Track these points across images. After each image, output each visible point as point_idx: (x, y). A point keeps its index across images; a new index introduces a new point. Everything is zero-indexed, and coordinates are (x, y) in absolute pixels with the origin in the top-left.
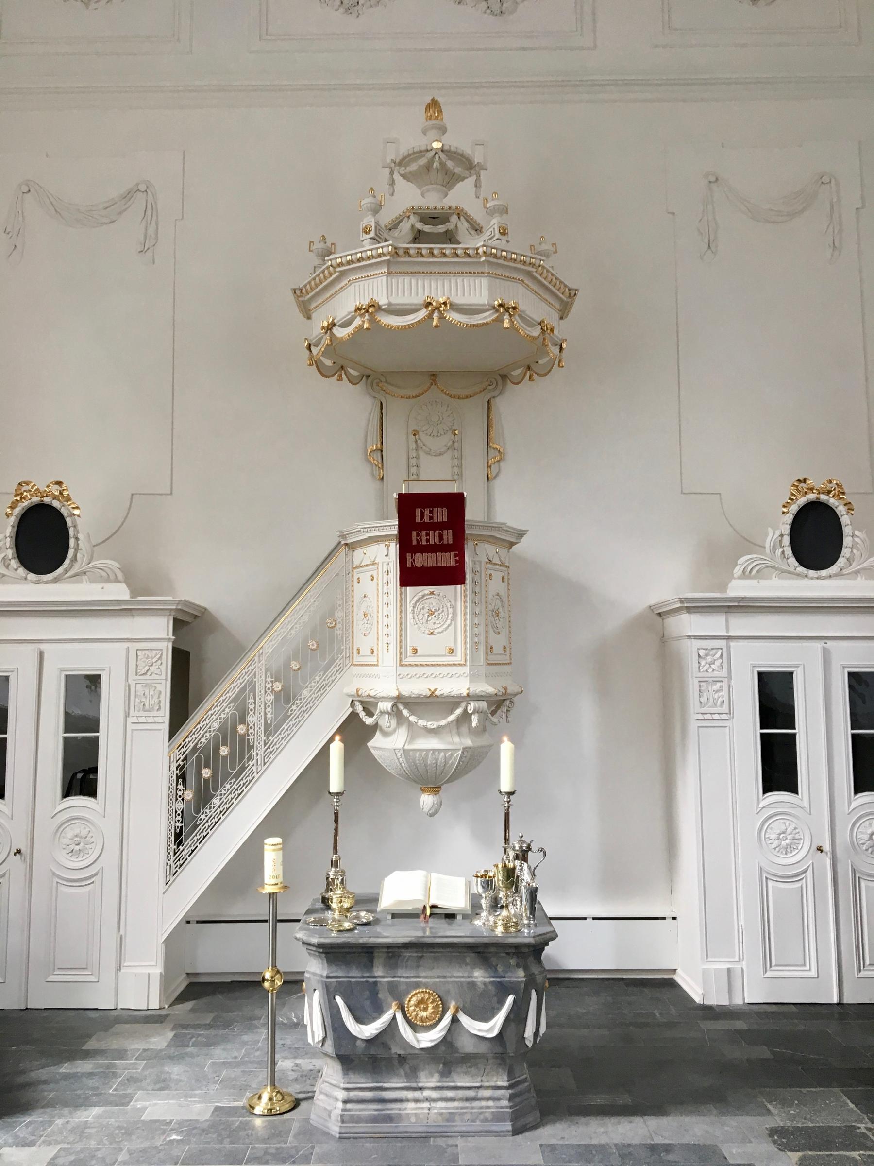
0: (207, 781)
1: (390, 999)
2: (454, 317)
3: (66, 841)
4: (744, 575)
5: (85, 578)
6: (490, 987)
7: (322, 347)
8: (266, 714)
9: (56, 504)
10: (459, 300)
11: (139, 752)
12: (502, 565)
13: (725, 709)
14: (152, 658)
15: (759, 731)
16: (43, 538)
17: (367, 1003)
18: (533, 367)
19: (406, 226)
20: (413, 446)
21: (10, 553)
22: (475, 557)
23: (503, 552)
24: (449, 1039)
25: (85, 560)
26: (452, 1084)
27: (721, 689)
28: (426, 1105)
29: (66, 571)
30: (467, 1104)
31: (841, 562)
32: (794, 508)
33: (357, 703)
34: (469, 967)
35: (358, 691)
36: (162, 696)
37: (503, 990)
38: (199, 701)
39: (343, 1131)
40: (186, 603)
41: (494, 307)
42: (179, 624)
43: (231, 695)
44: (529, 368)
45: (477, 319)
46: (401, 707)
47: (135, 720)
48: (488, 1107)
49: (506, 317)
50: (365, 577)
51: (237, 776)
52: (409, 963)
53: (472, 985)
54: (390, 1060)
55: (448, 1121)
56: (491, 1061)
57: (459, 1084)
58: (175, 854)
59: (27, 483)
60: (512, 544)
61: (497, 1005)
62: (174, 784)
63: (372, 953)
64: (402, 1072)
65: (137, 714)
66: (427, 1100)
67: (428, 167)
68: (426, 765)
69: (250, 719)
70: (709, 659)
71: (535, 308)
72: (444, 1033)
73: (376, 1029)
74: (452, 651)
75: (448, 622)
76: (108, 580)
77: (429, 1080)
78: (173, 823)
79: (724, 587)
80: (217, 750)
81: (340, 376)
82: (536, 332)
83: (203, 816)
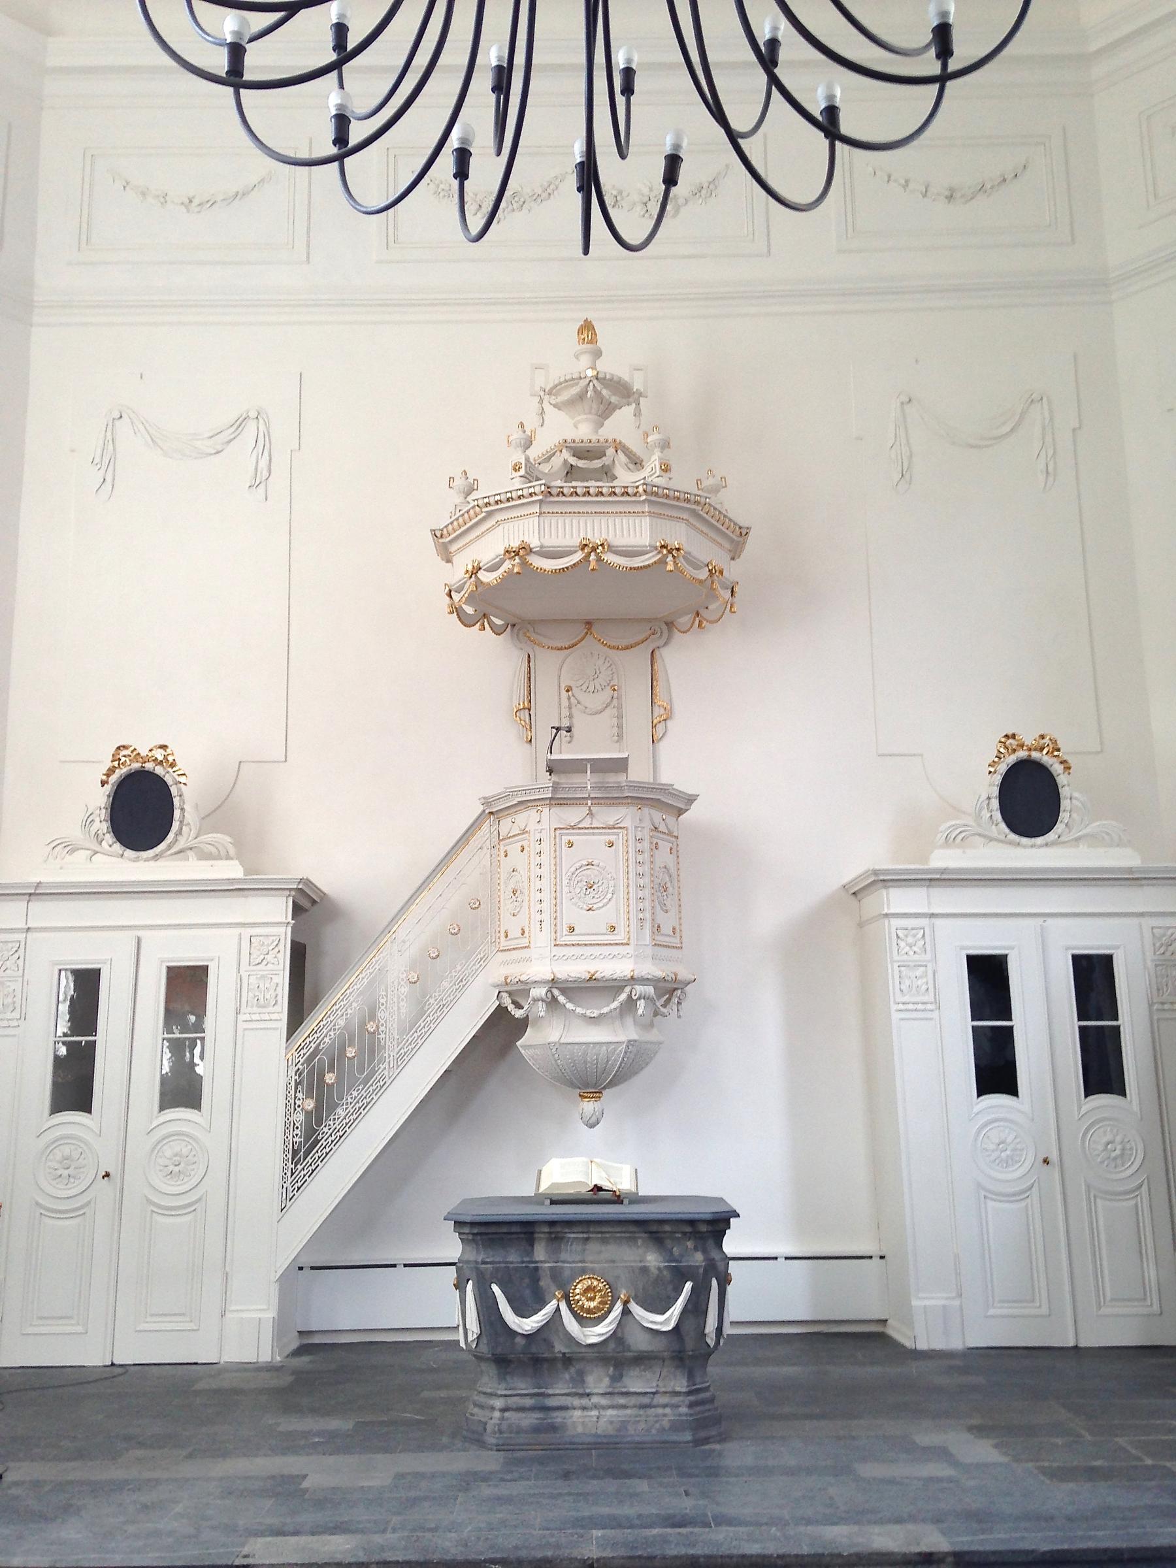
0: (331, 1086)
1: (553, 1288)
3: (161, 1161)
4: (948, 842)
5: (190, 854)
6: (665, 1273)
7: (465, 593)
8: (399, 1008)
9: (159, 770)
10: (618, 541)
12: (670, 834)
13: (930, 997)
14: (268, 945)
15: (970, 1024)
16: (141, 808)
17: (527, 1293)
18: (702, 611)
19: (557, 461)
20: (565, 703)
21: (105, 826)
23: (671, 820)
24: (619, 1335)
25: (193, 834)
26: (624, 1390)
27: (925, 975)
28: (594, 1413)
29: (169, 847)
30: (642, 1412)
31: (1059, 827)
32: (1003, 768)
33: (505, 995)
34: (641, 1251)
35: (506, 978)
36: (279, 989)
37: (680, 1275)
38: (315, 1003)
39: (501, 1442)
40: (307, 882)
41: (656, 548)
42: (297, 909)
44: (698, 614)
45: (638, 562)
46: (556, 992)
47: (247, 1017)
48: (665, 1415)
49: (670, 558)
50: (514, 849)
51: (366, 1082)
52: (574, 1246)
53: (644, 1270)
54: (552, 1361)
55: (619, 1430)
56: (667, 1363)
57: (632, 1390)
58: (292, 1174)
59: (125, 747)
60: (680, 812)
61: (673, 1295)
62: (293, 1092)
63: (533, 1233)
64: (567, 1376)
65: (249, 1010)
66: (596, 1407)
67: (582, 396)
68: (585, 1062)
70: (910, 940)
71: (703, 548)
72: (614, 1326)
73: (538, 1322)
74: (613, 928)
75: (609, 896)
76: (218, 857)
77: (598, 1381)
78: (290, 1137)
79: (926, 859)
80: (342, 1050)
81: (483, 625)
82: (703, 574)
83: (326, 1130)
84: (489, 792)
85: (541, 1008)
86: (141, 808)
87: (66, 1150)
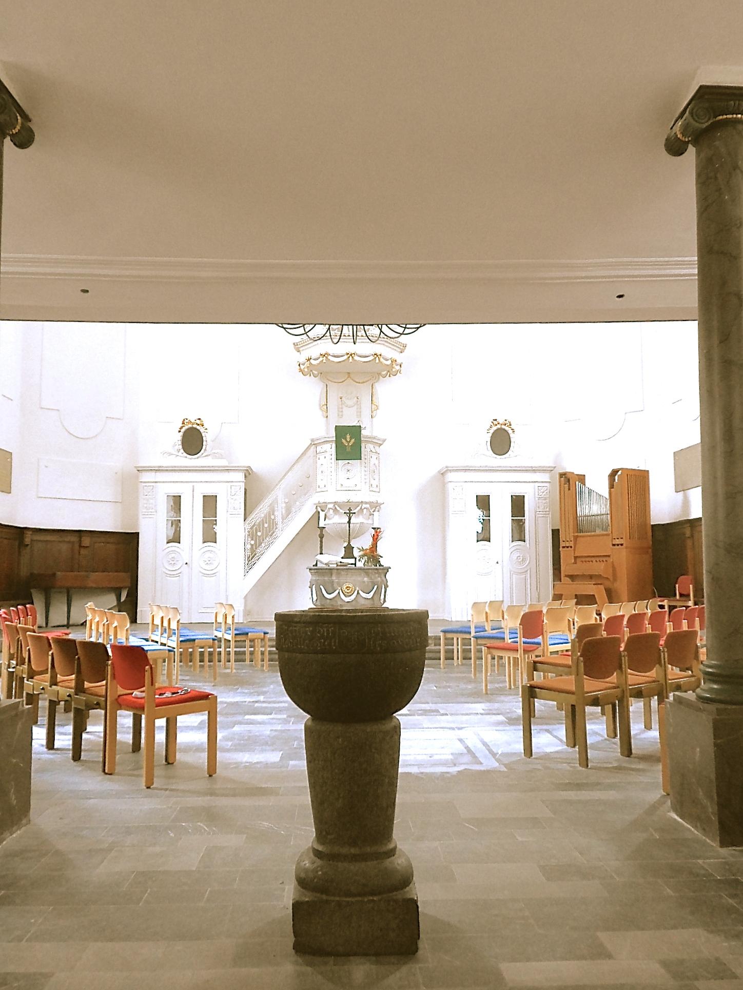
2: (356, 358)
5: (210, 457)
9: (198, 427)
10: (358, 352)
11: (232, 527)
16: (192, 441)
22: (366, 449)
23: (377, 448)
32: (492, 431)
43: (268, 504)
50: (322, 457)
69: (276, 513)
84: (314, 437)
85: (331, 511)
86: (192, 441)
87: (173, 555)
